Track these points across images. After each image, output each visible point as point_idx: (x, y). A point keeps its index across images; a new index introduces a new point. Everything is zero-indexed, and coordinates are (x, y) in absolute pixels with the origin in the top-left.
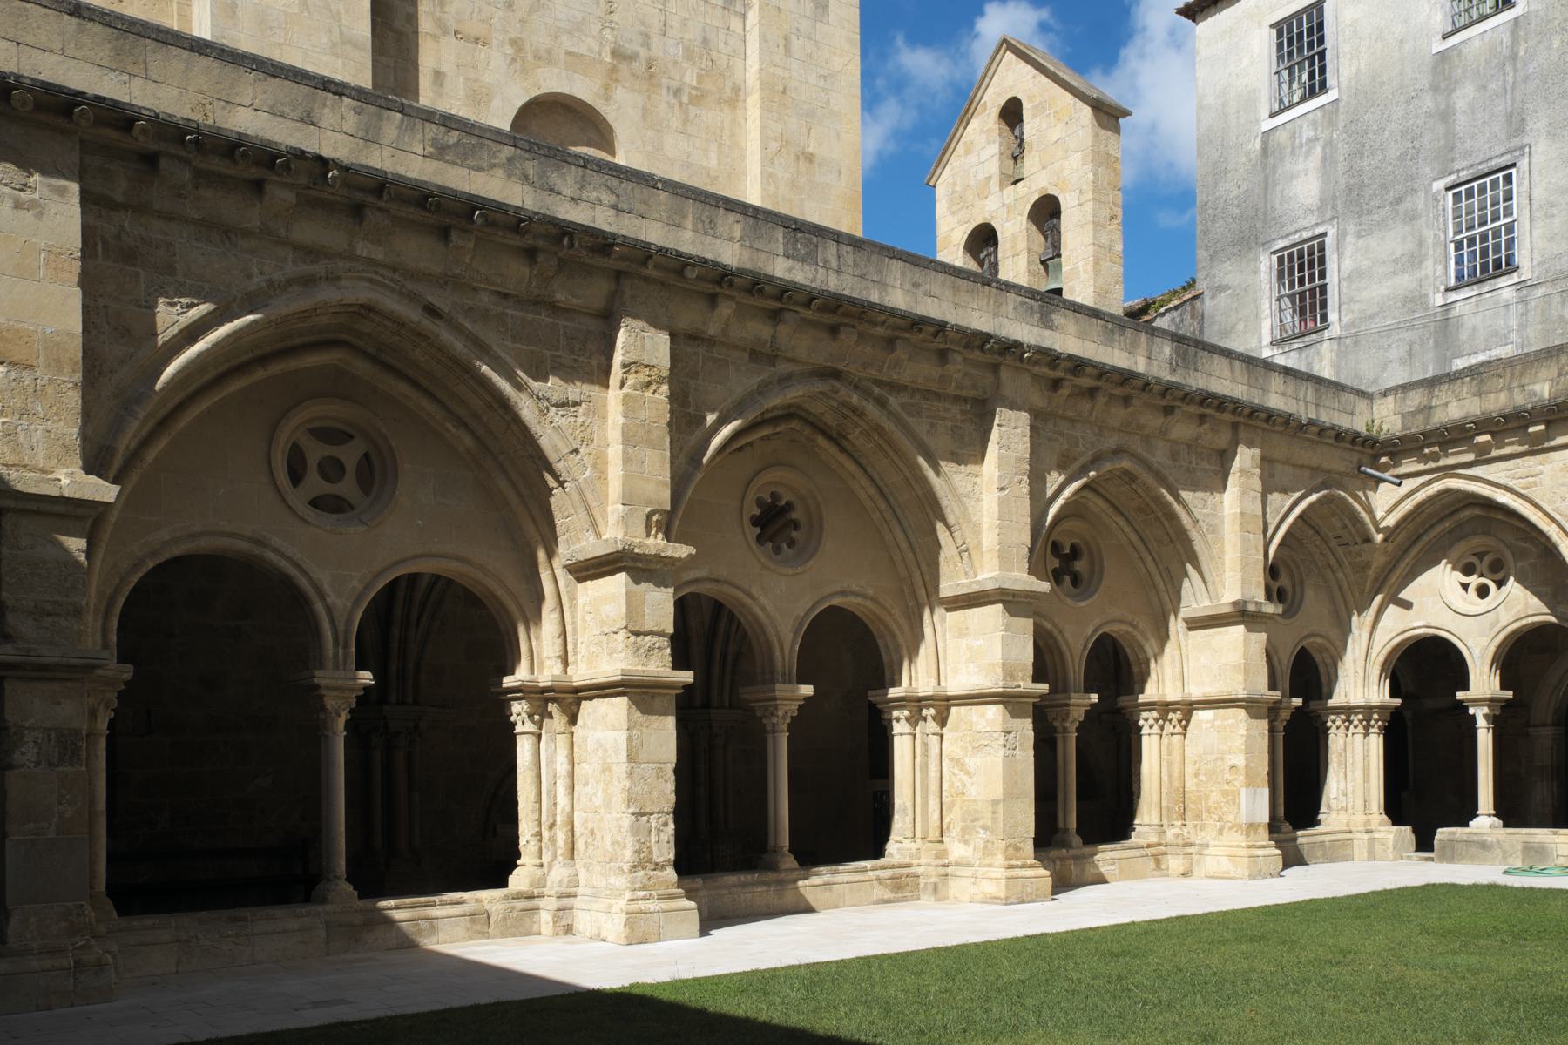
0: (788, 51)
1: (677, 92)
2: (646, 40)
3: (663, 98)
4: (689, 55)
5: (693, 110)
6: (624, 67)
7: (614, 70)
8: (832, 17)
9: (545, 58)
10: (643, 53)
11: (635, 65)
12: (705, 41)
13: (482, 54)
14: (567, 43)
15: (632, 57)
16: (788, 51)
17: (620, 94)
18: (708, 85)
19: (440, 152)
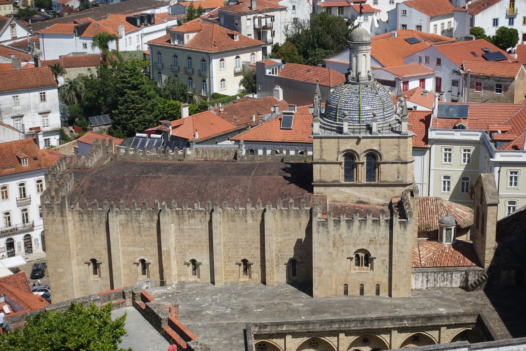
0: (398, 238)
1: (380, 244)
2: (375, 238)
3: (378, 246)
4: (383, 238)
5: (383, 246)
6: (371, 243)
7: (370, 243)
8: (407, 230)
9: (359, 244)
10: (375, 240)
11: (373, 242)
12: (385, 235)
13: (349, 246)
14: (362, 242)
15: (373, 240)
16: (398, 238)
17: (370, 246)
18: (385, 242)
19: (320, 325)
